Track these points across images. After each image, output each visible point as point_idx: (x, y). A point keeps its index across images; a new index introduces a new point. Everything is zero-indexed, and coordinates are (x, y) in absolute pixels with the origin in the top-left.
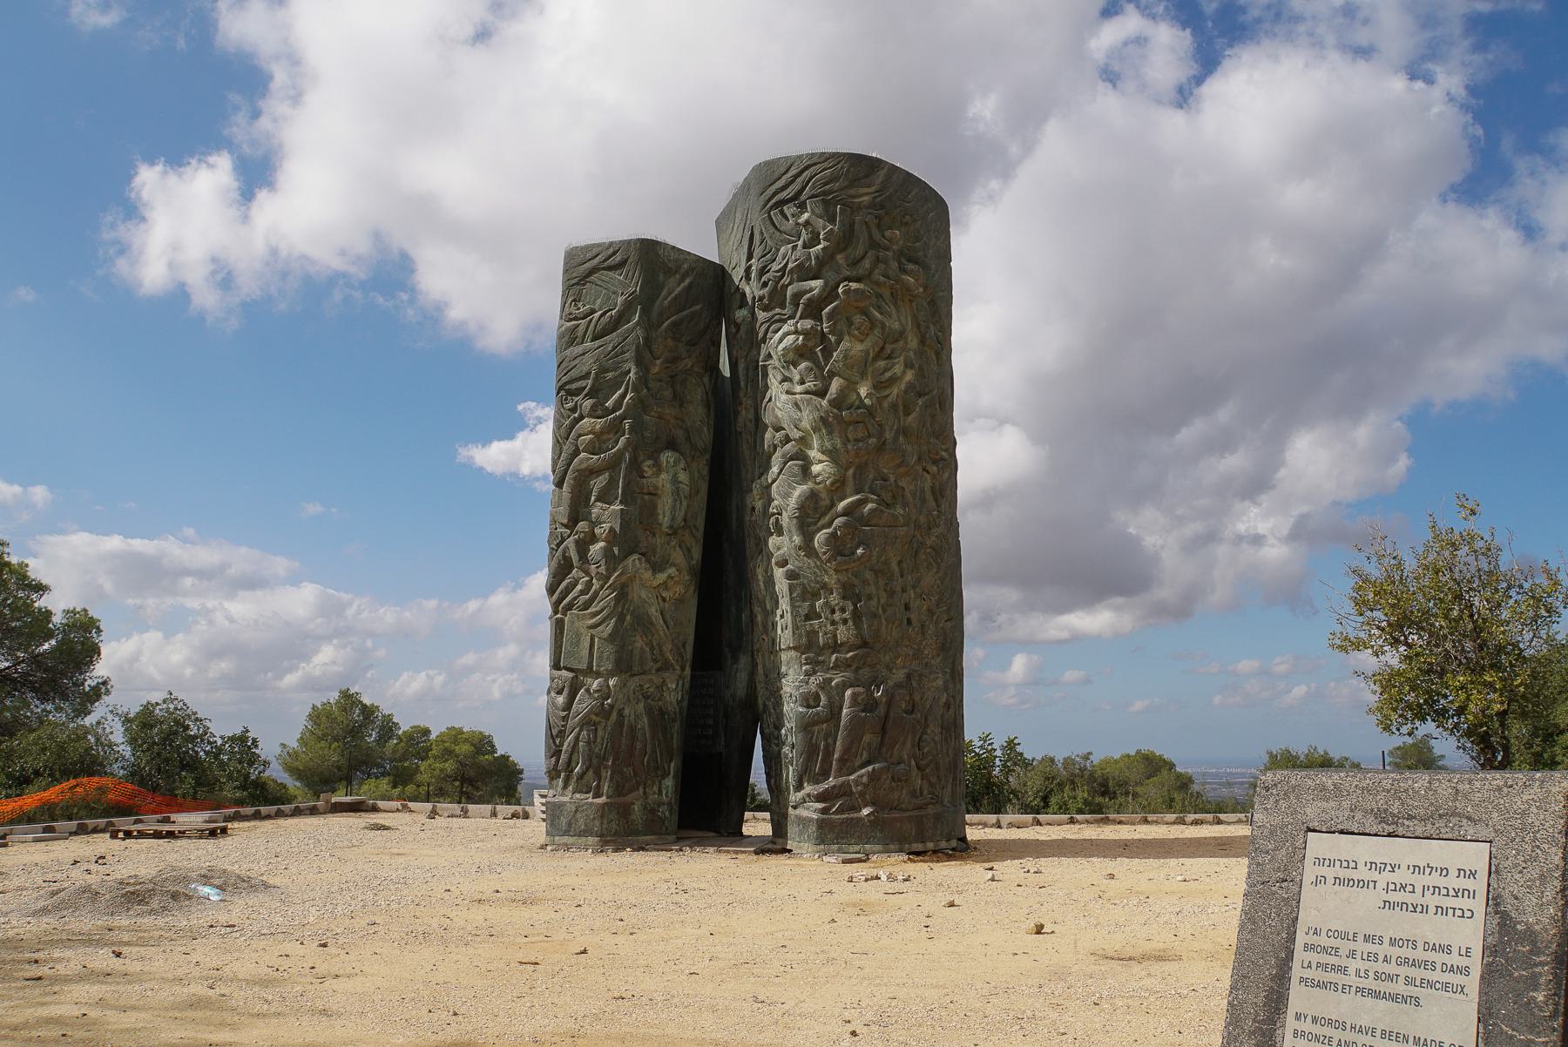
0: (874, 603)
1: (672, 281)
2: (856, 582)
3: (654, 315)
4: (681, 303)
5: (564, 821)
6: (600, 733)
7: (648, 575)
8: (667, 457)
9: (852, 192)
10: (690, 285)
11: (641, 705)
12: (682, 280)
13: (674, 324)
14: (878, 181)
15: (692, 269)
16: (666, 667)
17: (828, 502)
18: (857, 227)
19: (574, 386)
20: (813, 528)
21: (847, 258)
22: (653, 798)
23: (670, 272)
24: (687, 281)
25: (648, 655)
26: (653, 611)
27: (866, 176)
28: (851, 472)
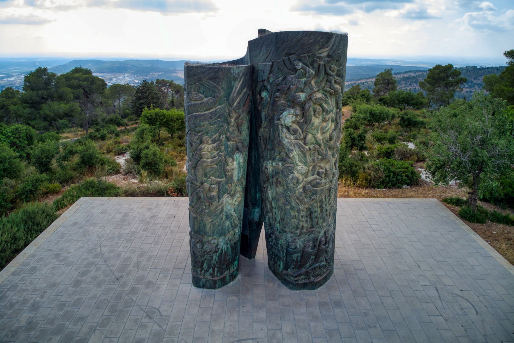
0: (316, 214)
1: (237, 82)
2: (310, 207)
3: (231, 101)
4: (239, 93)
5: (201, 284)
6: (214, 257)
7: (230, 201)
8: (237, 156)
9: (320, 51)
10: (243, 82)
11: (229, 245)
12: (240, 81)
13: (238, 103)
14: (331, 45)
15: (243, 74)
16: (234, 227)
17: (302, 180)
18: (321, 68)
19: (197, 129)
20: (295, 189)
21: (315, 83)
22: (232, 271)
23: (236, 79)
24: (242, 80)
25: (230, 226)
26: (232, 212)
27: (327, 43)
28: (311, 168)
